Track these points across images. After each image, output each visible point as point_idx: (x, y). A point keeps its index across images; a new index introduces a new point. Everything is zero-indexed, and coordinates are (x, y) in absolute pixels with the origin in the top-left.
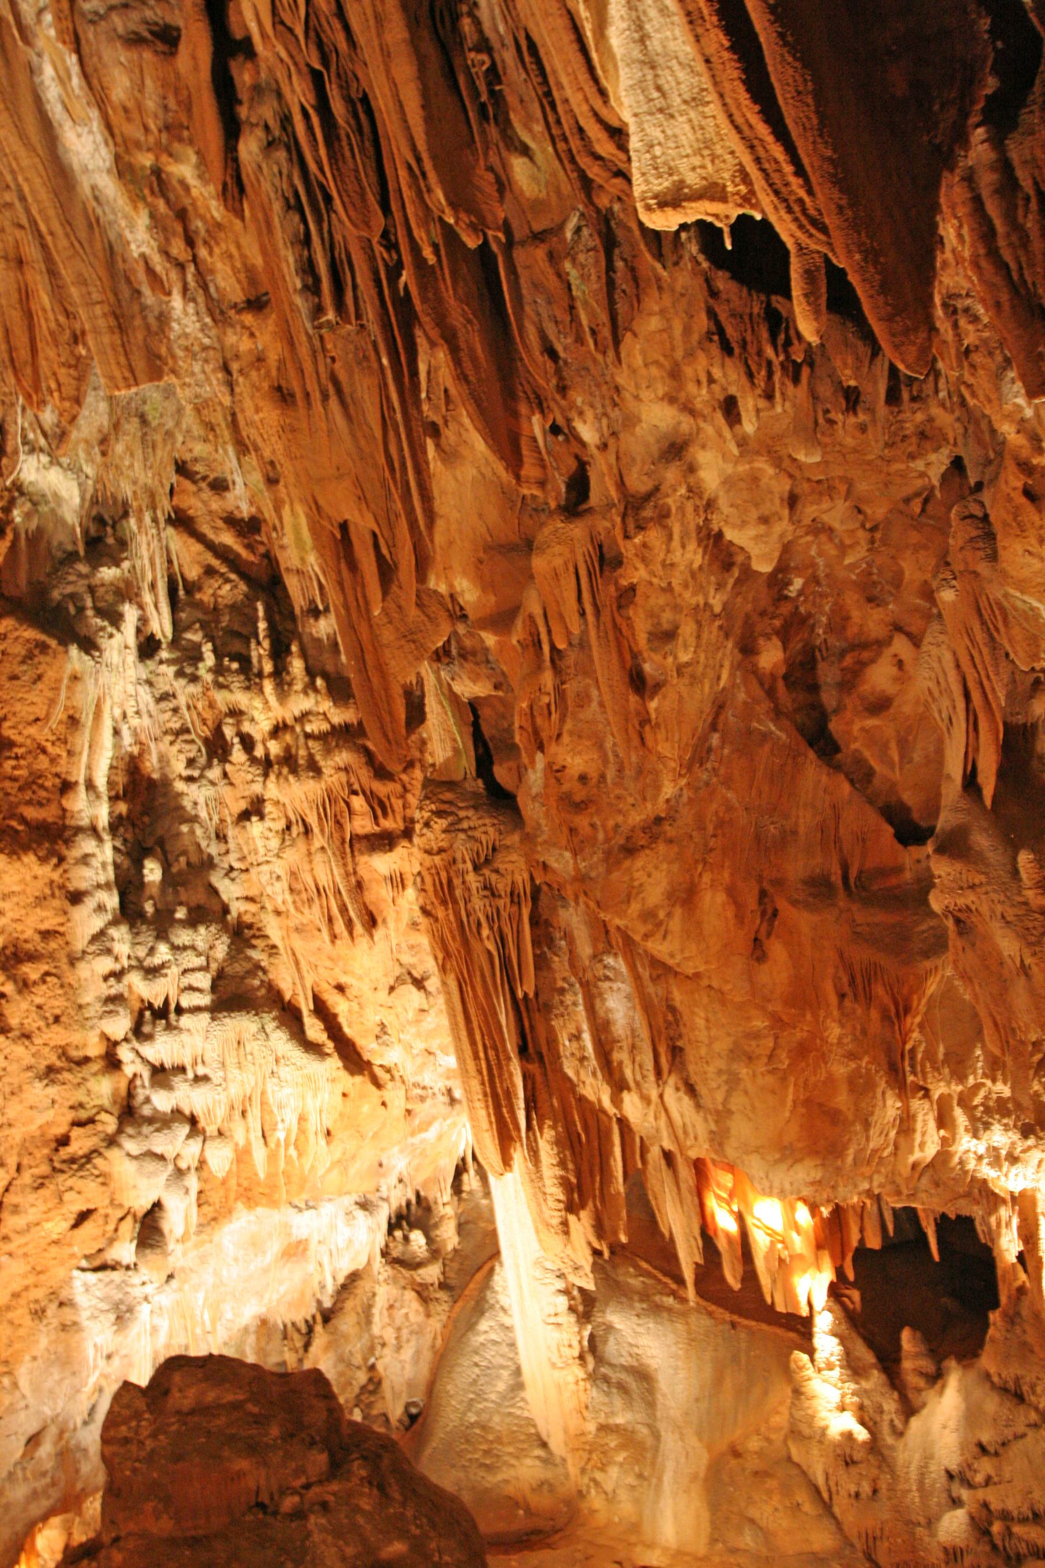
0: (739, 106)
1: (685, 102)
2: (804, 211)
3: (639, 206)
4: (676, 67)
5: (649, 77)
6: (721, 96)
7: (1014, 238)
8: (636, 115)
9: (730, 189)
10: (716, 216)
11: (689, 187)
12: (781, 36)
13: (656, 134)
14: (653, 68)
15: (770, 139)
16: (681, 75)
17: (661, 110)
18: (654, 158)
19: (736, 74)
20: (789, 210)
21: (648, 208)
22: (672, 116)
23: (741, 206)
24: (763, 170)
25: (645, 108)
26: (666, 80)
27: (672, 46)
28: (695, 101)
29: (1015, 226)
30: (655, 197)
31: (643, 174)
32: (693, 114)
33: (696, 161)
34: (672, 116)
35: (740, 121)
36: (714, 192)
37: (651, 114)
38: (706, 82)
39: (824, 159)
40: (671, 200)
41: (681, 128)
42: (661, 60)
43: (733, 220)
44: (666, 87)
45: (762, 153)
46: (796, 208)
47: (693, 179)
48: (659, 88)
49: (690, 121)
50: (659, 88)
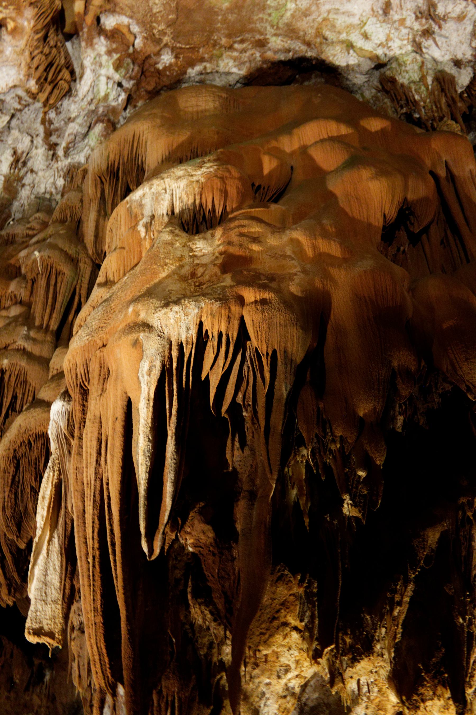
0: (100, 641)
1: (52, 601)
2: (108, 680)
3: (26, 631)
4: (53, 588)
5: (44, 588)
6: (96, 636)
7: (158, 709)
8: (36, 599)
9: (57, 636)
10: (49, 644)
11: (44, 630)
12: (129, 639)
13: (40, 607)
14: (46, 585)
15: (105, 655)
16: (54, 591)
17: (44, 601)
18: (37, 615)
19: (102, 632)
20: (104, 679)
21: (29, 633)
22: (46, 604)
23: (58, 643)
24: (101, 663)
25: (39, 598)
26: (49, 591)
27: (54, 581)
28: (55, 602)
29: (159, 705)
30: (33, 629)
31: (31, 620)
32: (53, 606)
33: (49, 622)
34: (46, 604)
35: (99, 645)
36: (51, 635)
37: (41, 600)
38: (60, 597)
39: (130, 678)
40: (38, 632)
41: (48, 609)
42: (49, 584)
43: (54, 647)
44: (48, 593)
45: (102, 658)
46: (106, 679)
47: (46, 628)
48: (45, 593)
49: (52, 608)
50: (45, 593)
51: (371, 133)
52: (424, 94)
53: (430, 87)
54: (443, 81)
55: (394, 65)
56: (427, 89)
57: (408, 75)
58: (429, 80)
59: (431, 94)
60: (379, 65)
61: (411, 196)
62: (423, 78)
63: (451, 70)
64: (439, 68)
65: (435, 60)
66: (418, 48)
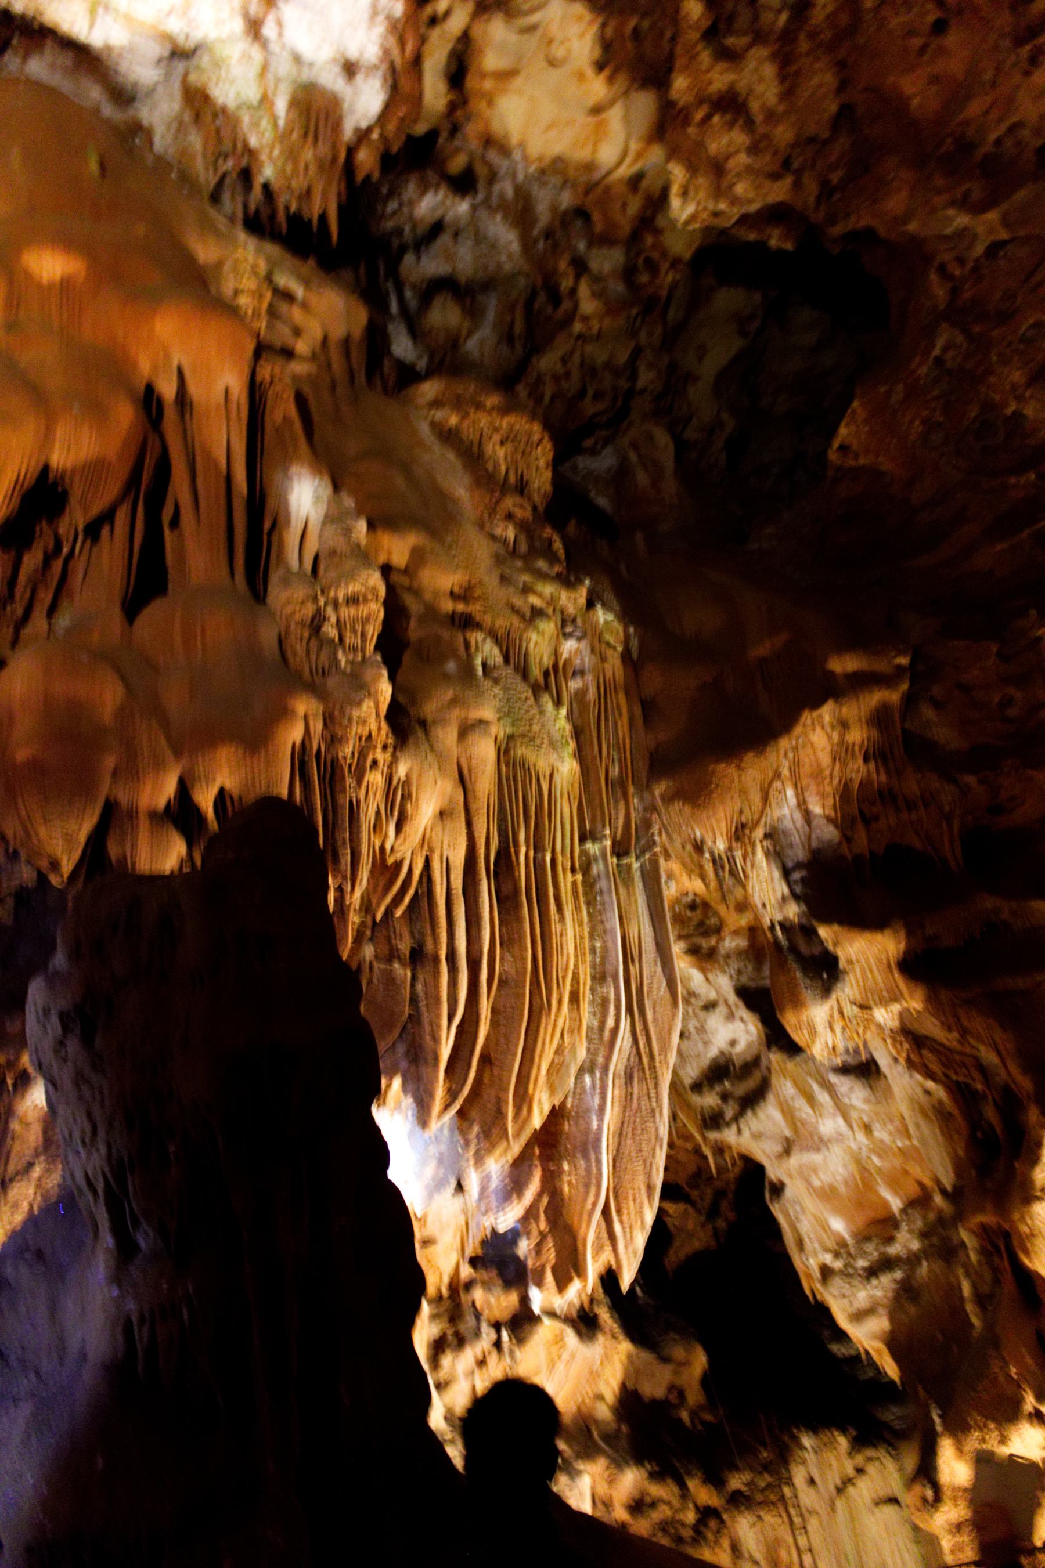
51: (40, 286)
52: (269, 136)
53: (281, 122)
54: (314, 109)
55: (205, 61)
56: (275, 125)
57: (235, 83)
58: (281, 105)
59: (283, 137)
60: (179, 53)
61: (58, 458)
62: (266, 101)
63: (332, 80)
64: (306, 76)
65: (297, 59)
66: (254, 28)
